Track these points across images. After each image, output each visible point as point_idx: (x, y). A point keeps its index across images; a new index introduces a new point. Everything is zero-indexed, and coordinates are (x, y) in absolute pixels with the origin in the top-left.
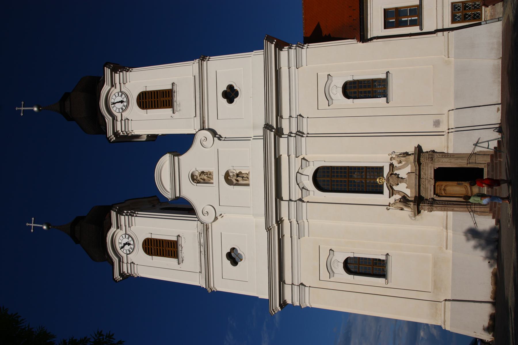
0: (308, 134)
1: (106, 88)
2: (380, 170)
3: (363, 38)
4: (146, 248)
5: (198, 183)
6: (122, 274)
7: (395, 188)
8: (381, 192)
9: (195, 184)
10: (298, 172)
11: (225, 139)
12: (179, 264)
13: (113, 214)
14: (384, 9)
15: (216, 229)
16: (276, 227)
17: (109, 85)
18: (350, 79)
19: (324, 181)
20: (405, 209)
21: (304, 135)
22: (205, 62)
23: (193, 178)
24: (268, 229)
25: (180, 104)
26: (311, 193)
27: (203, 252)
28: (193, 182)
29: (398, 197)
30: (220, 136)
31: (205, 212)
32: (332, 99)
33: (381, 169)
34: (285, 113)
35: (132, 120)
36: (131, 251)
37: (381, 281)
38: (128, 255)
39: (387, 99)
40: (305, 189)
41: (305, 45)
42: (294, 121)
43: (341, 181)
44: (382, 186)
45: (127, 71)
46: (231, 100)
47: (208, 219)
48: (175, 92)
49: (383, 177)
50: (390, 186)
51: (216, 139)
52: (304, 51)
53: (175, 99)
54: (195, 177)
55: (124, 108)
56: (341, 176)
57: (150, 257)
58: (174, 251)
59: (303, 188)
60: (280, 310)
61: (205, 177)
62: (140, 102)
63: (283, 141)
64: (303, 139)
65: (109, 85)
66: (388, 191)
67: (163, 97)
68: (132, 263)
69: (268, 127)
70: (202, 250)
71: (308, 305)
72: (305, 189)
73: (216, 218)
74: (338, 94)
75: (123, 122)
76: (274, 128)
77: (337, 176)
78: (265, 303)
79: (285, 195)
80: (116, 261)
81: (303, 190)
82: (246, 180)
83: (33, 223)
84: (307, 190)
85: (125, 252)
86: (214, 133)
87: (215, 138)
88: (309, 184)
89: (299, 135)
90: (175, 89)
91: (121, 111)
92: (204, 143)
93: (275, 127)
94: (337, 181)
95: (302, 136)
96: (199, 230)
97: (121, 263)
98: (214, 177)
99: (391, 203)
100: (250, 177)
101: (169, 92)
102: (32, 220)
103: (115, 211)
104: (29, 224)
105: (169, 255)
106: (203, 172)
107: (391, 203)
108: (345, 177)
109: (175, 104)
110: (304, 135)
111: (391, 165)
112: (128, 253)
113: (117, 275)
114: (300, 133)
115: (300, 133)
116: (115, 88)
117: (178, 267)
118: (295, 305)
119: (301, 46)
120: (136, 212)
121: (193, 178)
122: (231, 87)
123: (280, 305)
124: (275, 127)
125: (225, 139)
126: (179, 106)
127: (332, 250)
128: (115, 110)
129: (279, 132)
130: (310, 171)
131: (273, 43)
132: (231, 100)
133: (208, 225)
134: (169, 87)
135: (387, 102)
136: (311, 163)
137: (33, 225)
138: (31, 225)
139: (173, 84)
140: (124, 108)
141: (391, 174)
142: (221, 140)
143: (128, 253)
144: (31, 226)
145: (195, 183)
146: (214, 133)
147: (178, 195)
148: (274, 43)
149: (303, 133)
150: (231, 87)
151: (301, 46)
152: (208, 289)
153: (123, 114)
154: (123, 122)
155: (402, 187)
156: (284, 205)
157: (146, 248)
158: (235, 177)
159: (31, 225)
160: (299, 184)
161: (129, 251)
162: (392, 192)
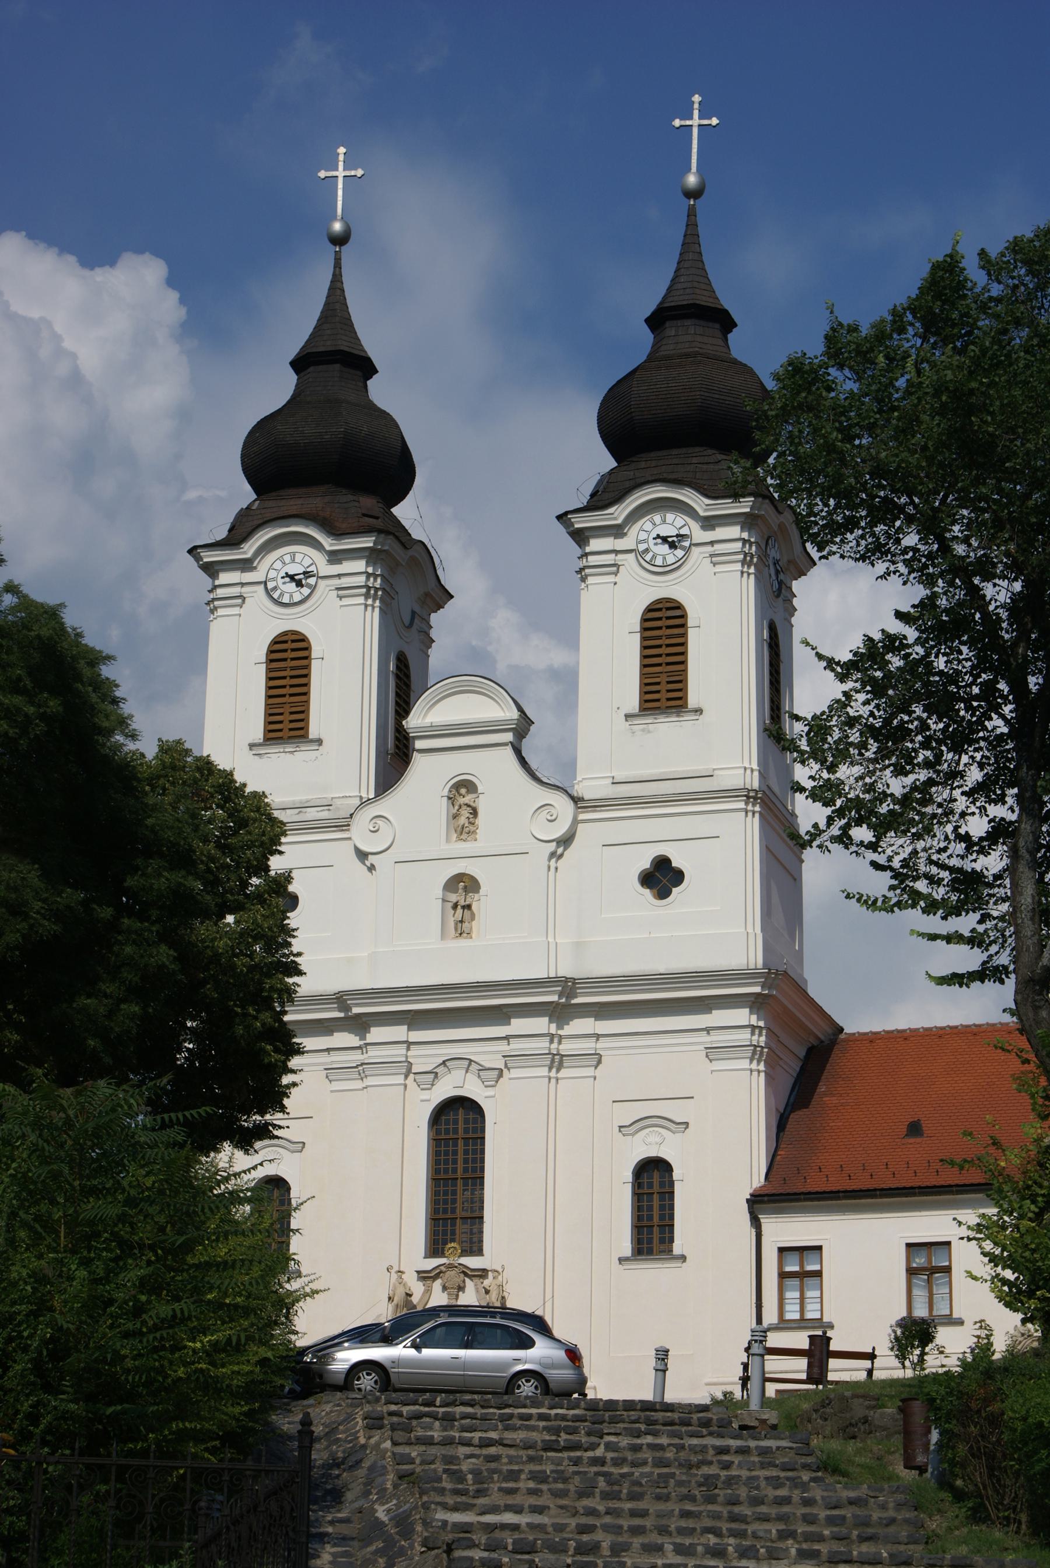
0: (557, 1079)
1: (700, 503)
2: (475, 1248)
4: (286, 642)
7: (437, 1285)
9: (446, 792)
10: (471, 1061)
11: (552, 869)
12: (252, 746)
13: (367, 542)
14: (819, 1248)
17: (706, 510)
18: (676, 1175)
19: (456, 1122)
20: (391, 1307)
21: (554, 1070)
22: (742, 805)
23: (464, 786)
25: (649, 732)
26: (425, 1095)
28: (452, 787)
29: (418, 1289)
30: (561, 856)
31: (380, 822)
33: (480, 1252)
35: (615, 584)
36: (276, 596)
38: (263, 586)
39: (627, 1259)
41: (762, 1064)
42: (588, 1046)
43: (455, 1162)
44: (443, 1255)
45: (743, 562)
46: (647, 879)
47: (360, 835)
48: (678, 716)
49: (459, 1257)
50: (441, 1272)
52: (745, 1064)
54: (463, 791)
55: (648, 558)
56: (466, 1161)
57: (261, 654)
58: (280, 730)
59: (436, 1073)
61: (462, 820)
62: (660, 610)
63: (541, 1024)
64: (544, 1071)
66: (429, 1268)
67: (668, 682)
68: (244, 599)
69: (569, 986)
73: (362, 855)
74: (646, 1146)
75: (609, 559)
77: (466, 1152)
80: (244, 553)
81: (432, 1076)
82: (456, 929)
83: (348, 173)
84: (433, 1085)
85: (270, 576)
86: (566, 841)
87: (554, 844)
88: (445, 1089)
89: (553, 1061)
91: (642, 547)
92: (544, 814)
94: (455, 1153)
95: (550, 1069)
96: (338, 802)
98: (462, 845)
99: (403, 1276)
100: (463, 942)
101: (680, 698)
102: (356, 169)
103: (375, 543)
104: (341, 158)
105: (271, 715)
106: (475, 812)
107: (403, 1276)
108: (465, 1170)
110: (554, 1070)
111: (483, 1273)
112: (270, 585)
113: (209, 557)
115: (557, 1061)
120: (377, 603)
121: (464, 786)
122: (678, 877)
125: (552, 869)
126: (643, 730)
128: (644, 528)
130: (473, 1089)
131: (763, 987)
132: (647, 879)
133: (348, 830)
134: (692, 701)
135: (621, 1260)
136: (490, 1092)
137: (341, 173)
138: (341, 165)
139: (699, 711)
140: (648, 558)
142: (549, 860)
143: (270, 585)
144: (337, 169)
145: (450, 791)
146: (566, 841)
147: (419, 744)
149: (558, 1071)
150: (678, 877)
153: (631, 557)
156: (399, 1032)
157: (286, 642)
158: (462, 903)
159: (341, 165)
160: (445, 1066)
161: (275, 588)
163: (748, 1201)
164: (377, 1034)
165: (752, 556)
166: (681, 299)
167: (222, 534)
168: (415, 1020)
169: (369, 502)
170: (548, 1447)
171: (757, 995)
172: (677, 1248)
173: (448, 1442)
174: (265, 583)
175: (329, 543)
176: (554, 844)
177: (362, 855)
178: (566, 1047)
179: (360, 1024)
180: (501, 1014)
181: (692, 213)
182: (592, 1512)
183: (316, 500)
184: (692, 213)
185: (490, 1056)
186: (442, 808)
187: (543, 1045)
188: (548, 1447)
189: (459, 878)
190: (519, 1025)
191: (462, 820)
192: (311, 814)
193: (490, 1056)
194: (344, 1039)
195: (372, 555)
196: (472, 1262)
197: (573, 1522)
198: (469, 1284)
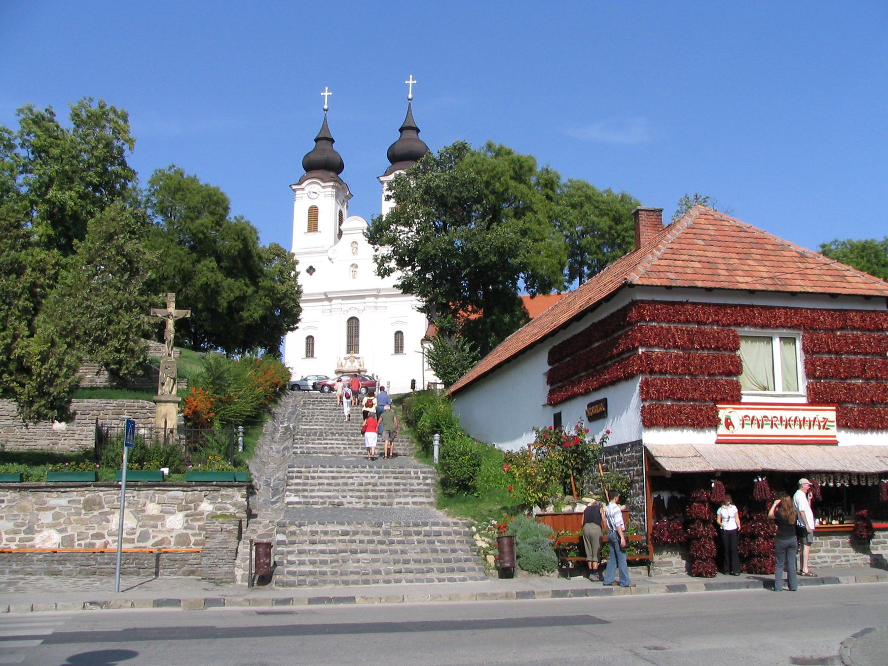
2: (357, 352)
3: (423, 341)
8: (348, 352)
13: (332, 184)
24: (325, 294)
37: (304, 355)
42: (384, 304)
61: (354, 251)
63: (373, 299)
69: (379, 290)
73: (330, 259)
111: (359, 358)
113: (294, 187)
141: (355, 358)
155: (349, 364)
156: (340, 301)
162: (345, 359)
164: (334, 301)
166: (405, 126)
167: (298, 182)
168: (343, 298)
169: (332, 174)
170: (334, 410)
172: (404, 352)
173: (313, 409)
175: (323, 184)
177: (330, 259)
178: (379, 305)
179: (330, 300)
180: (363, 297)
181: (410, 104)
182: (332, 426)
183: (319, 173)
184: (410, 104)
185: (361, 307)
186: (350, 248)
187: (373, 304)
188: (334, 410)
189: (353, 265)
190: (367, 299)
191: (354, 251)
192: (318, 249)
194: (326, 303)
195: (333, 187)
196: (356, 355)
197: (328, 428)
198: (356, 360)
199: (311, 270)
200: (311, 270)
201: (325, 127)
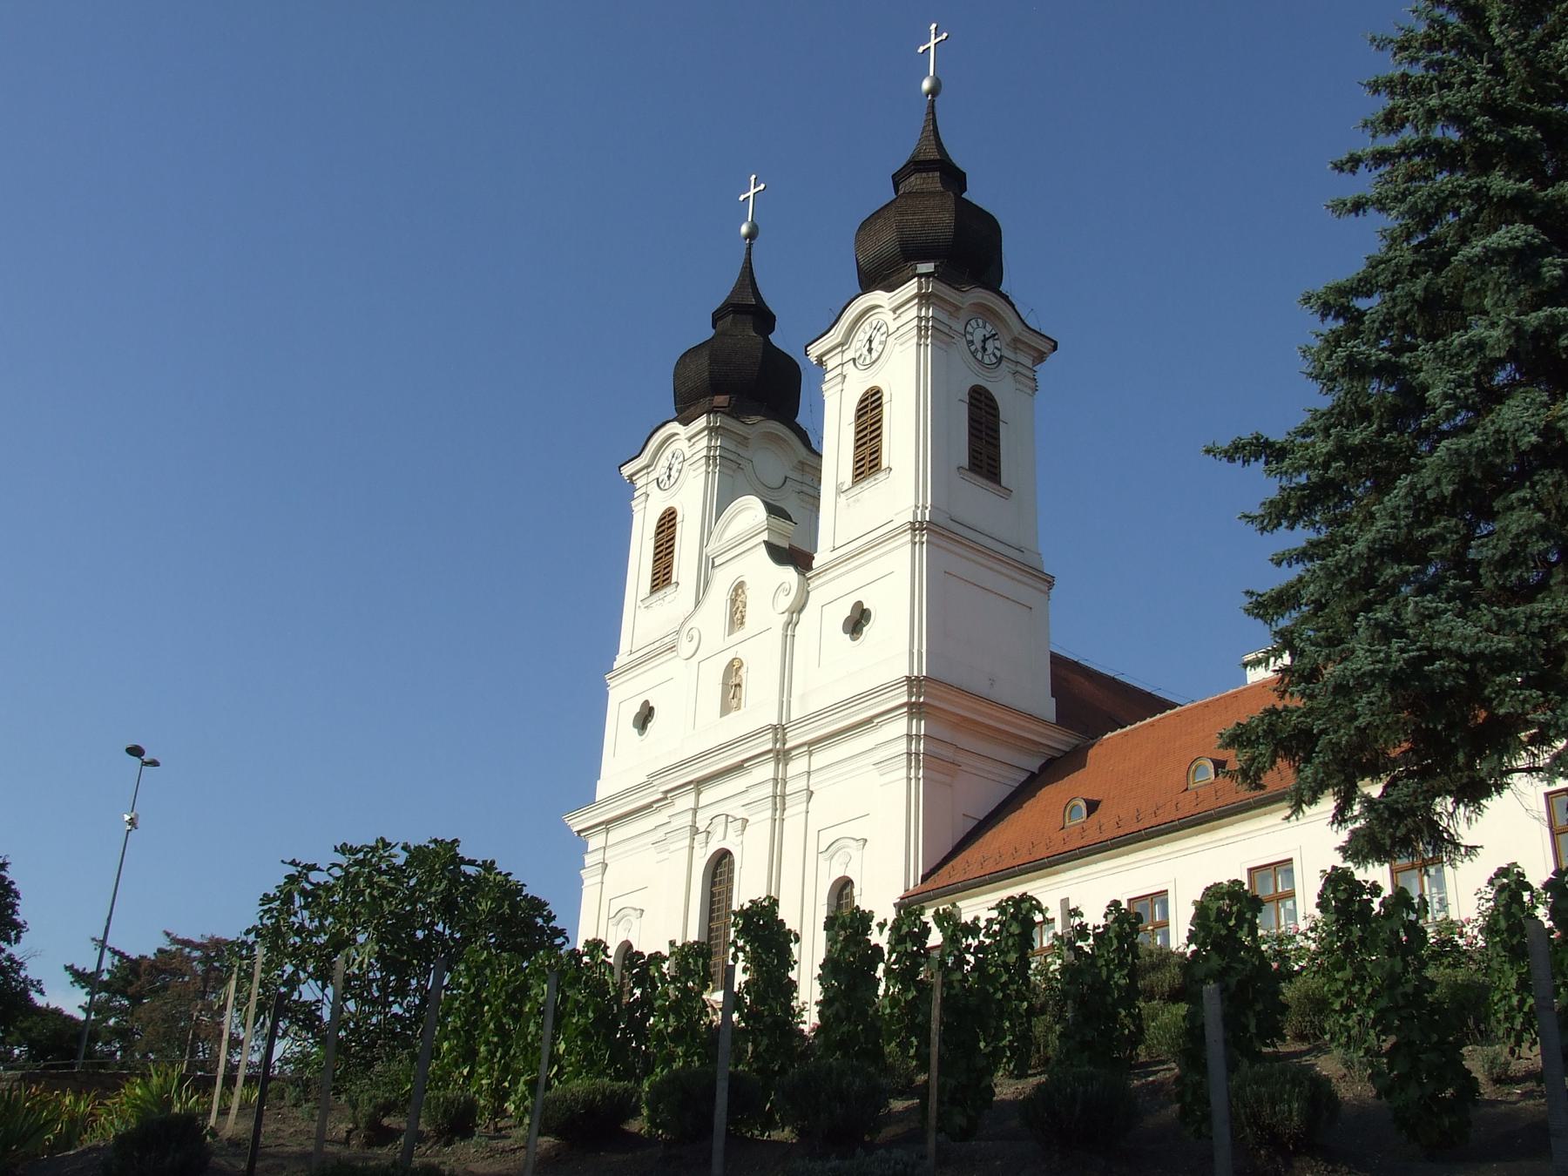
5: (732, 600)
6: (631, 476)
10: (727, 816)
15: (671, 667)
16: (660, 796)
27: (653, 647)
32: (832, 857)
34: (821, 758)
40: (707, 838)
51: (785, 617)
53: (864, 484)
60: (575, 829)
61: (738, 615)
62: (867, 398)
65: (890, 304)
70: (657, 645)
71: (586, 883)
72: (707, 838)
76: (784, 744)
78: (586, 798)
79: (710, 794)
84: (707, 843)
87: (787, 614)
88: (714, 846)
90: (881, 476)
92: (781, 595)
93: (787, 746)
97: (645, 471)
109: (857, 489)
113: (627, 471)
114: (779, 801)
115: (779, 801)
116: (895, 319)
117: (640, 598)
118: (586, 857)
119: (913, 764)
123: (579, 832)
124: (787, 746)
127: (642, 915)
129: (782, 756)
134: (884, 464)
146: (799, 608)
148: (913, 699)
151: (913, 764)
152: (607, 676)
154: (838, 370)
163: (895, 905)
165: (927, 328)
171: (909, 705)
174: (658, 479)
176: (787, 614)
193: (735, 808)
199: (645, 717)
200: (645, 717)
201: (748, 274)
